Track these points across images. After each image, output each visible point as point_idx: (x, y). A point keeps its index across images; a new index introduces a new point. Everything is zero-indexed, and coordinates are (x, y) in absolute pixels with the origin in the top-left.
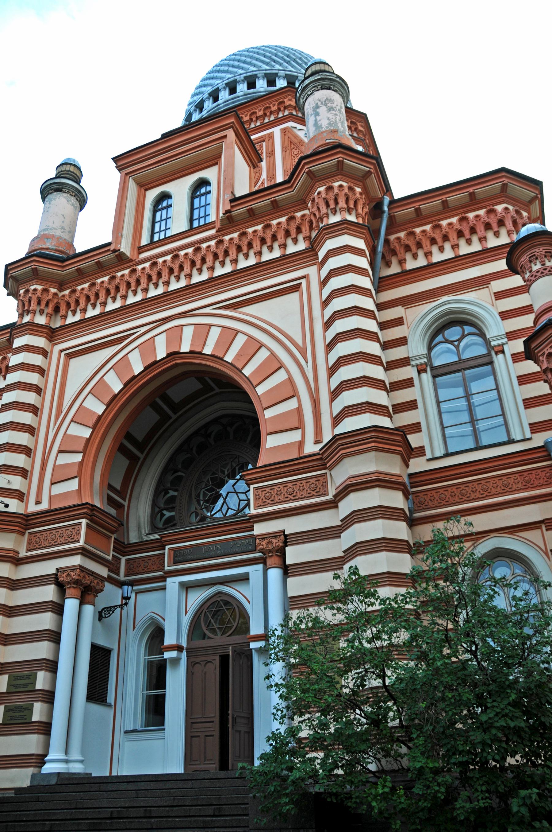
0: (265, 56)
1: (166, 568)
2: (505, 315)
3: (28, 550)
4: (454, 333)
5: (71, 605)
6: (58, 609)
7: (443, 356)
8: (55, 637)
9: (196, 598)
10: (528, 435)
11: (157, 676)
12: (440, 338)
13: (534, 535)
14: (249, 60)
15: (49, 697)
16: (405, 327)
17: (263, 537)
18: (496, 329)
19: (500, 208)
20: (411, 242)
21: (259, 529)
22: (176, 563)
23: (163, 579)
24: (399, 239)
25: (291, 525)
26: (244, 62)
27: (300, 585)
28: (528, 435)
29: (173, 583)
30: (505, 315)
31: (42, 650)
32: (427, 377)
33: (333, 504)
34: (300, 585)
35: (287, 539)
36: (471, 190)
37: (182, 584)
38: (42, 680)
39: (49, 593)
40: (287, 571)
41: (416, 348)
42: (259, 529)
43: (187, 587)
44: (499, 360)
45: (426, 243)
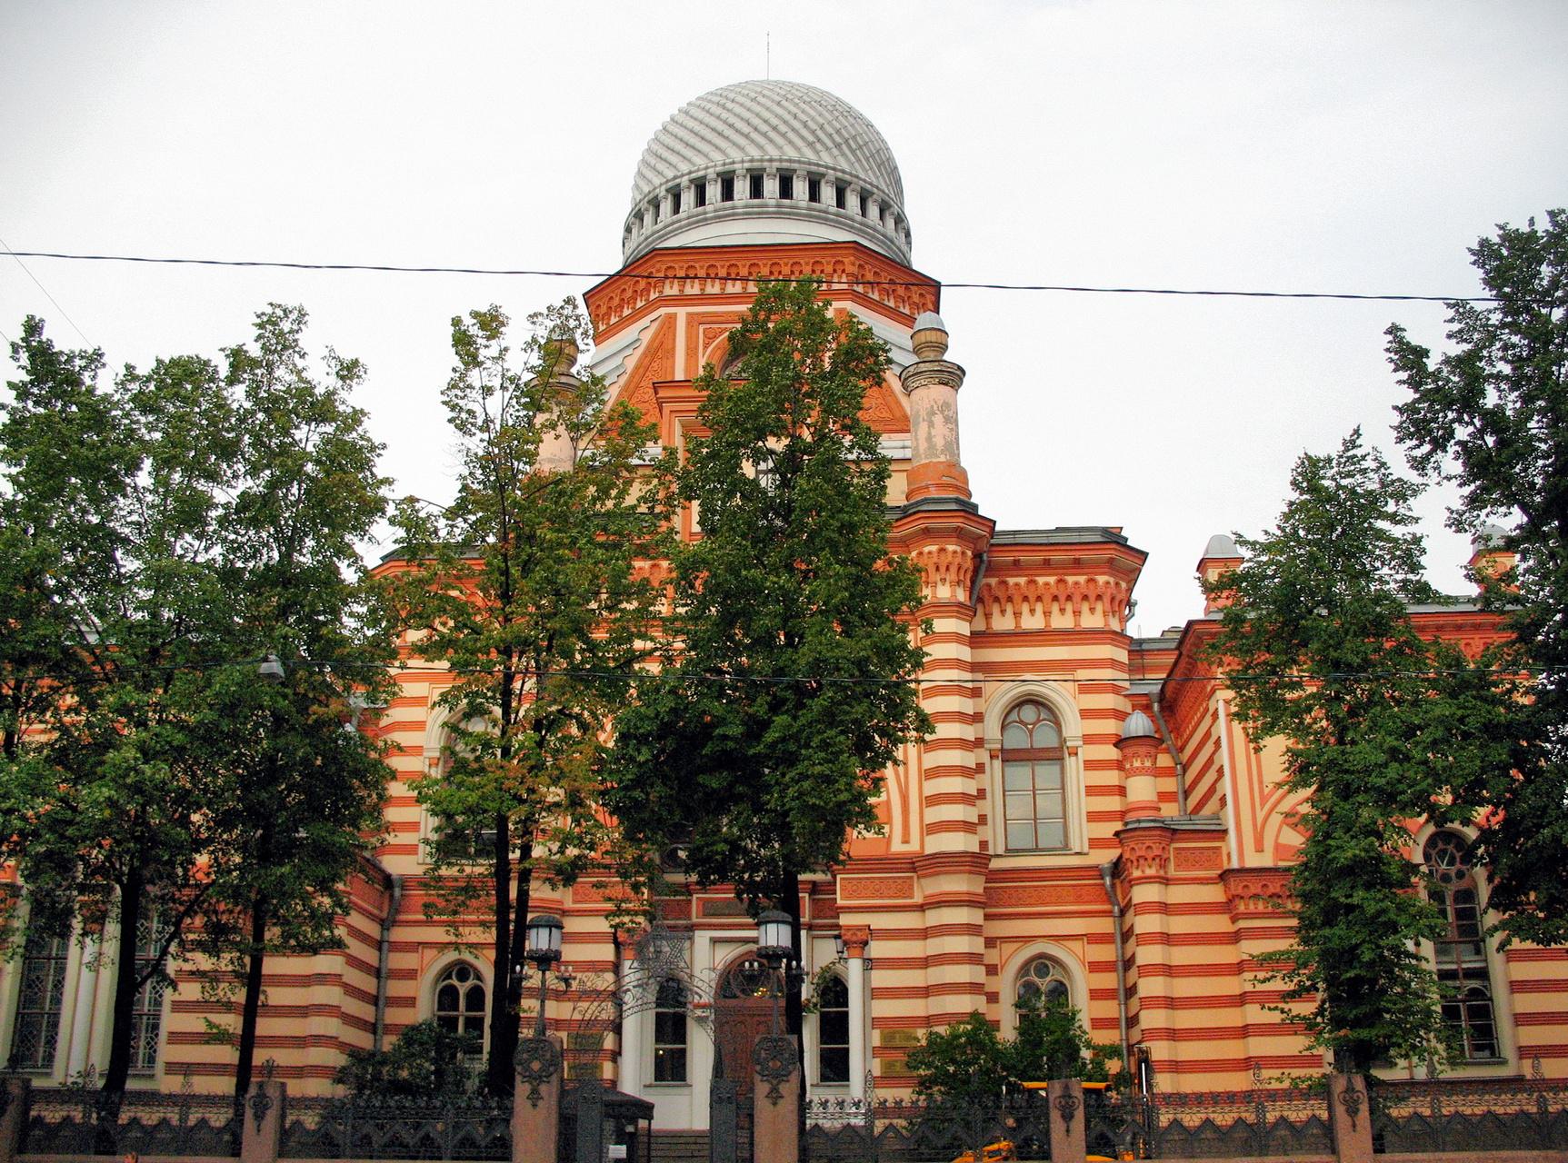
0: (805, 125)
1: (695, 920)
2: (1086, 714)
3: (575, 902)
4: (1029, 713)
5: (627, 965)
6: (616, 968)
7: (1017, 739)
8: (616, 997)
9: (725, 955)
10: (1086, 849)
11: (671, 1028)
12: (1014, 716)
13: (1076, 946)
14: (783, 128)
15: (616, 1055)
16: (982, 700)
17: (849, 928)
18: (1074, 728)
19: (1101, 579)
20: (1000, 594)
21: (845, 920)
22: (705, 915)
23: (692, 928)
24: (989, 585)
25: (879, 921)
26: (775, 128)
27: (881, 978)
28: (1086, 849)
29: (702, 937)
30: (1086, 714)
31: (608, 1011)
32: (997, 763)
33: (921, 908)
34: (881, 978)
35: (872, 933)
36: (1077, 555)
37: (714, 941)
38: (609, 1042)
39: (606, 952)
40: (870, 964)
41: (991, 729)
42: (845, 920)
43: (715, 941)
44: (1070, 762)
45: (1017, 599)
